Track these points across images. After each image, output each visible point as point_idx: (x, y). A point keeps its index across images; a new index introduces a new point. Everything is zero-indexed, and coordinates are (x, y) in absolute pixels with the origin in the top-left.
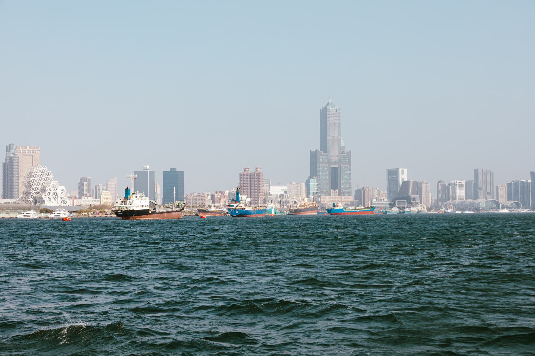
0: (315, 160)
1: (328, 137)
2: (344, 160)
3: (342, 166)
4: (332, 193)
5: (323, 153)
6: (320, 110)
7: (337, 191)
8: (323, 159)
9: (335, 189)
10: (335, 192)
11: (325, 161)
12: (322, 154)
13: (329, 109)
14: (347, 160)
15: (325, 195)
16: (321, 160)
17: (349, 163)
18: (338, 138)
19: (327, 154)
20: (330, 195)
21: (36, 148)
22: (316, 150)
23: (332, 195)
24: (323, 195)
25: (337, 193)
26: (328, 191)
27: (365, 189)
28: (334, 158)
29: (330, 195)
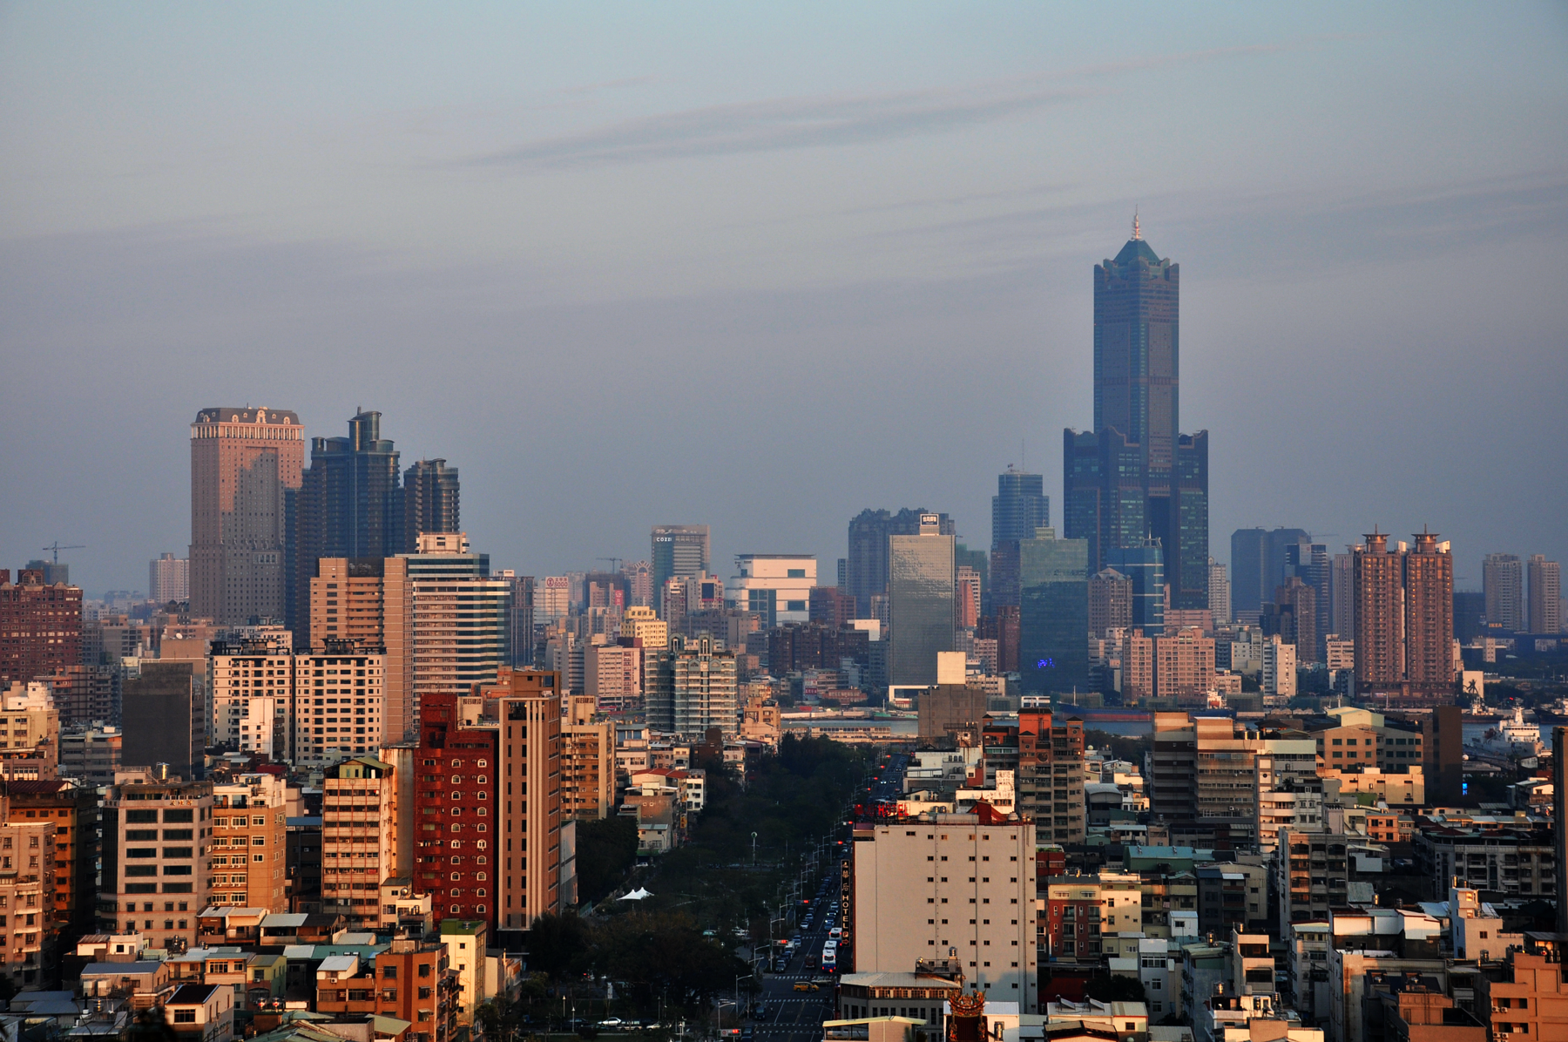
0: (1095, 469)
3: (1184, 492)
6: (1097, 268)
8: (1126, 465)
12: (1126, 445)
13: (1147, 269)
14: (1196, 471)
16: (1122, 469)
17: (1202, 481)
19: (1137, 445)
21: (287, 419)
28: (1159, 463)
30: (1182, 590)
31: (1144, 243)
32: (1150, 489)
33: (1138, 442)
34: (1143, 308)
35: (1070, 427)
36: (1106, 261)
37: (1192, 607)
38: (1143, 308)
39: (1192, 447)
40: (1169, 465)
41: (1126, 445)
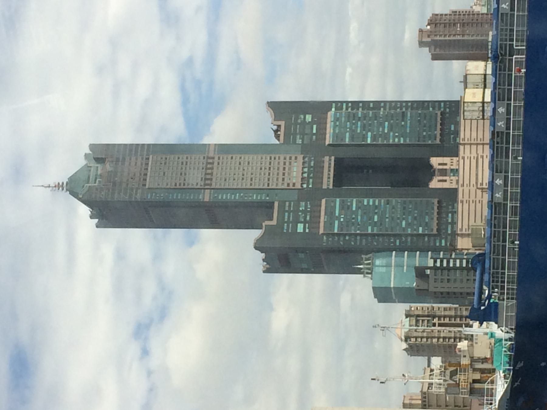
1: (207, 199)
2: (307, 131)
3: (329, 141)
4: (446, 185)
5: (271, 219)
7: (435, 161)
8: (297, 222)
9: (430, 172)
10: (443, 172)
11: (305, 212)
12: (274, 222)
14: (309, 118)
15: (454, 213)
18: (211, 154)
19: (276, 204)
20: (456, 190)
22: (256, 248)
23: (454, 186)
24: (454, 223)
25: (447, 160)
26: (435, 201)
27: (424, 40)
29: (456, 190)
30: (438, 141)
31: (71, 179)
32: (325, 187)
33: (273, 203)
34: (131, 195)
35: (261, 268)
36: (91, 217)
37: (457, 124)
38: (131, 195)
39: (282, 124)
40: (300, 157)
41: (274, 222)
